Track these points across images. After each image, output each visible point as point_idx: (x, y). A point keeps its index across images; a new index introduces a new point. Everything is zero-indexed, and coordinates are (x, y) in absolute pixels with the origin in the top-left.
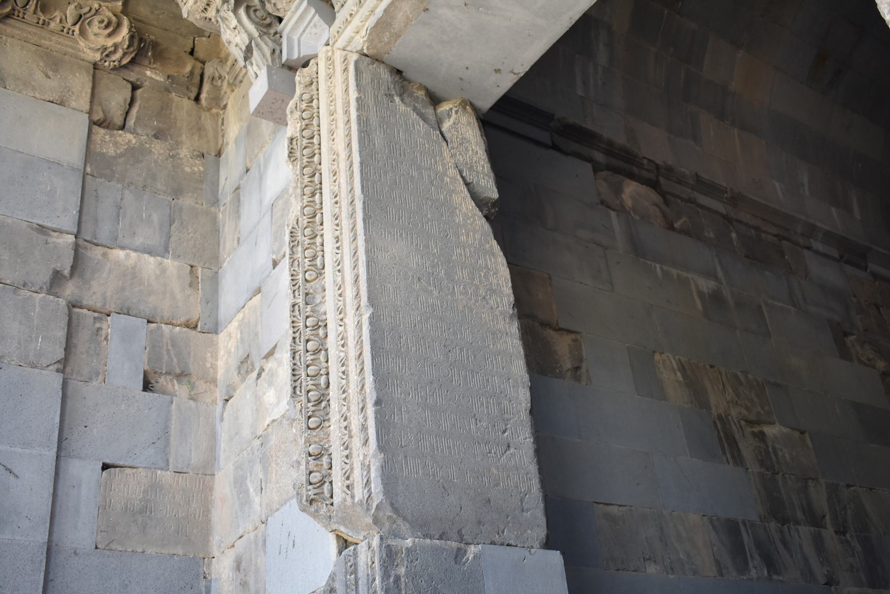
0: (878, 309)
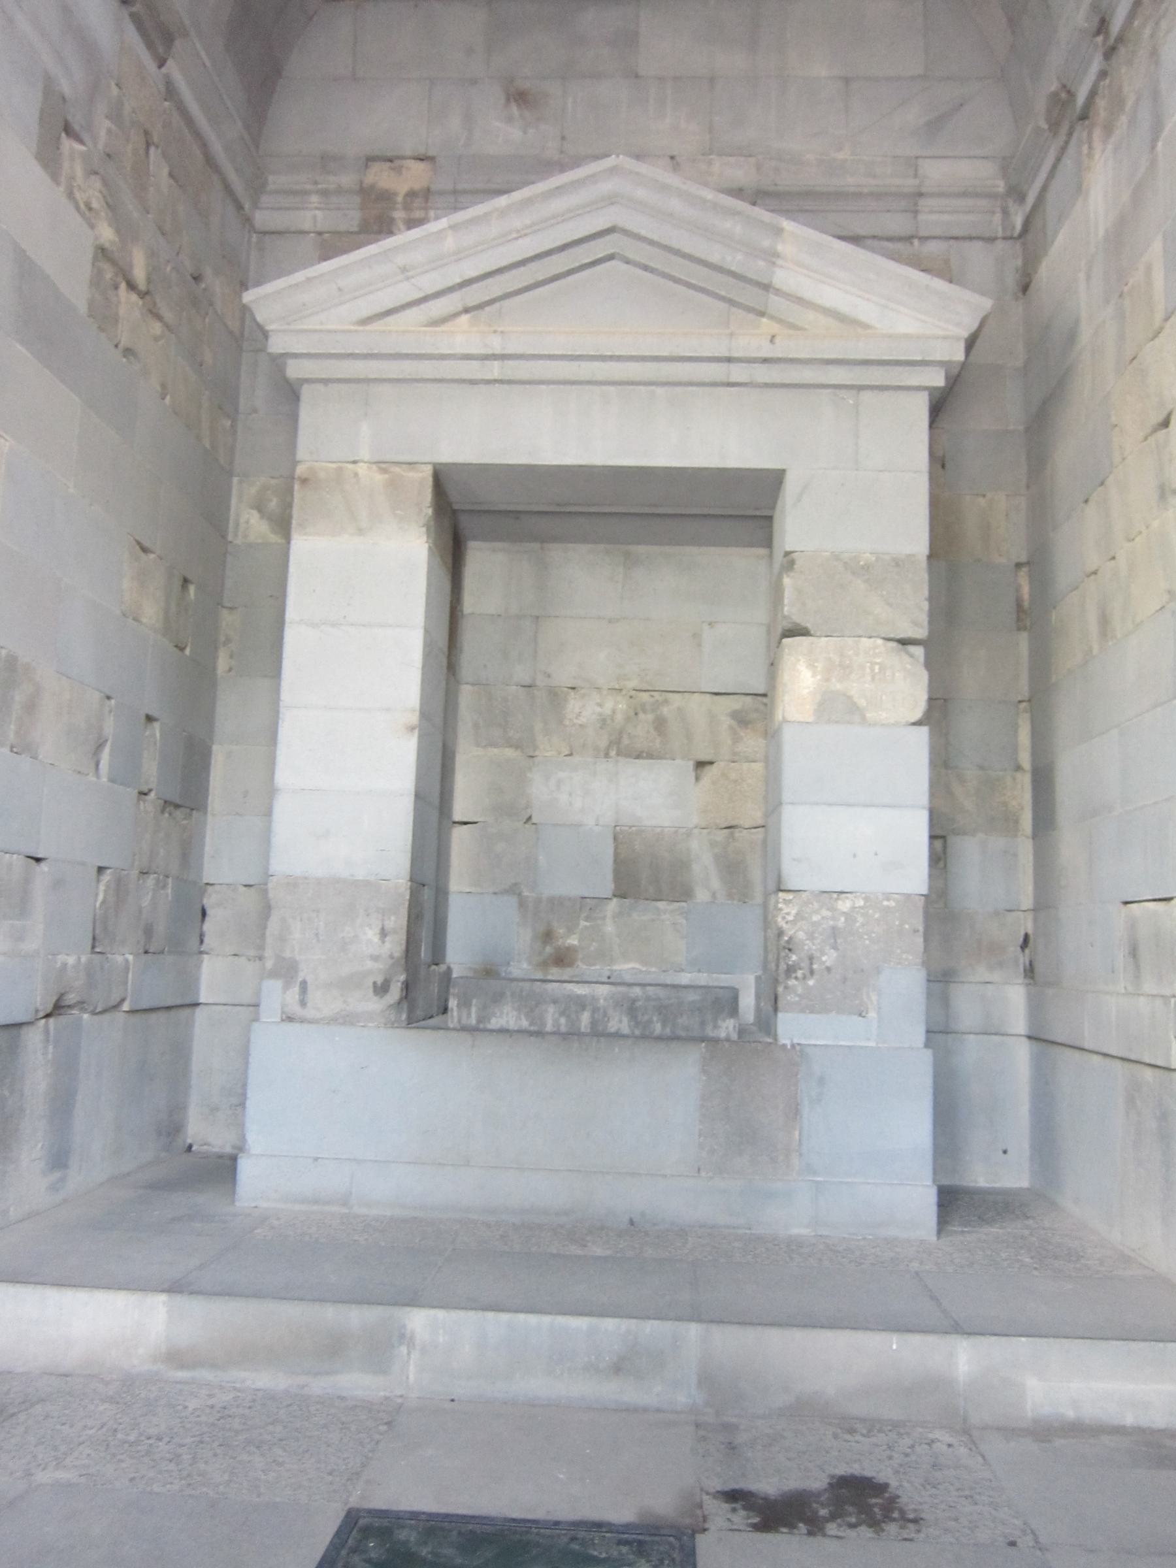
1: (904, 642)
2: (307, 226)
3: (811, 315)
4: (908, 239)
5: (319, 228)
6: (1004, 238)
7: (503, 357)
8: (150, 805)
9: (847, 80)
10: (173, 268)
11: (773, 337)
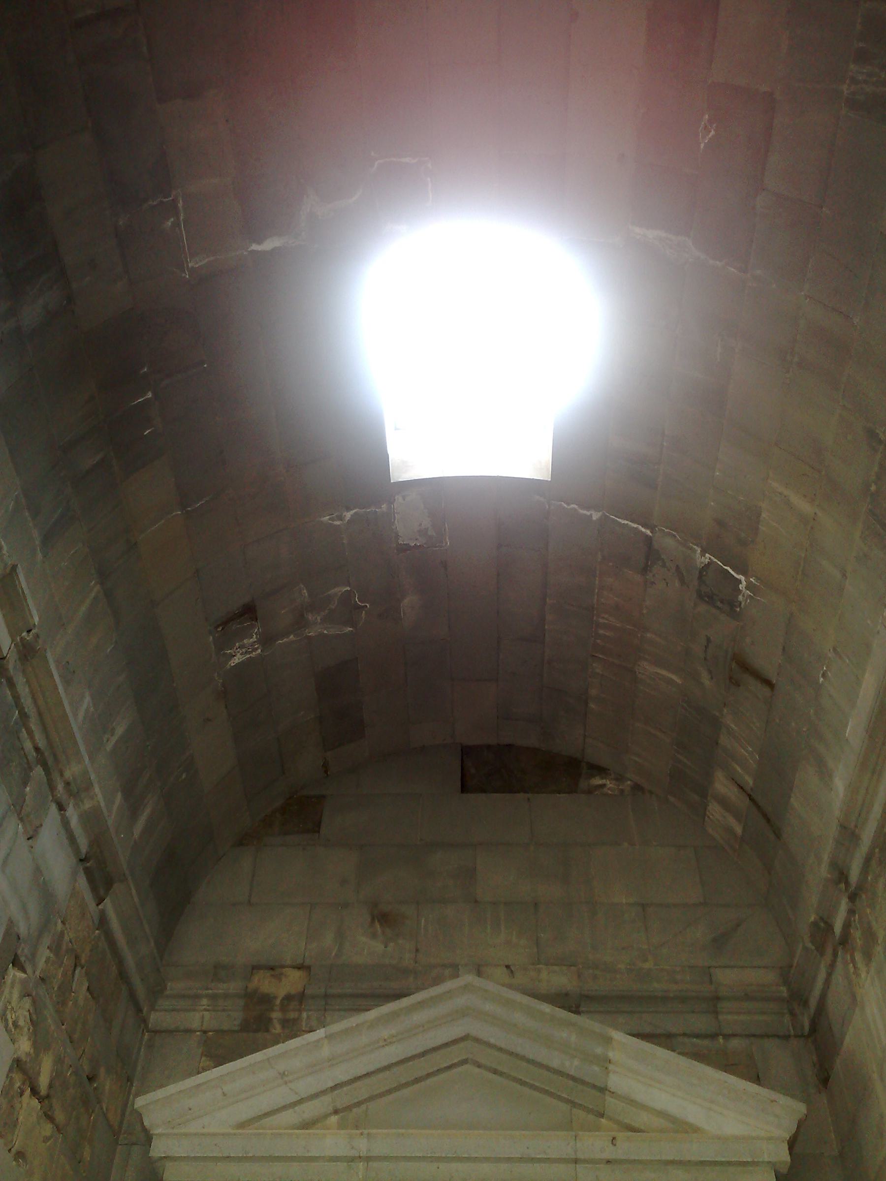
0: (76, 966)
2: (196, 1025)
4: (713, 1036)
5: (204, 1028)
6: (796, 1036)
7: (368, 1159)
9: (644, 906)
10: (73, 1072)
11: (614, 1138)
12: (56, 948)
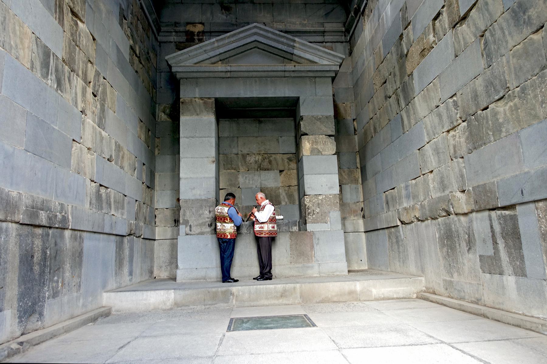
1: (330, 136)
2: (172, 40)
3: (303, 60)
4: (322, 42)
6: (345, 42)
7: (231, 72)
8: (144, 186)
9: (305, 4)
12: (132, 14)
